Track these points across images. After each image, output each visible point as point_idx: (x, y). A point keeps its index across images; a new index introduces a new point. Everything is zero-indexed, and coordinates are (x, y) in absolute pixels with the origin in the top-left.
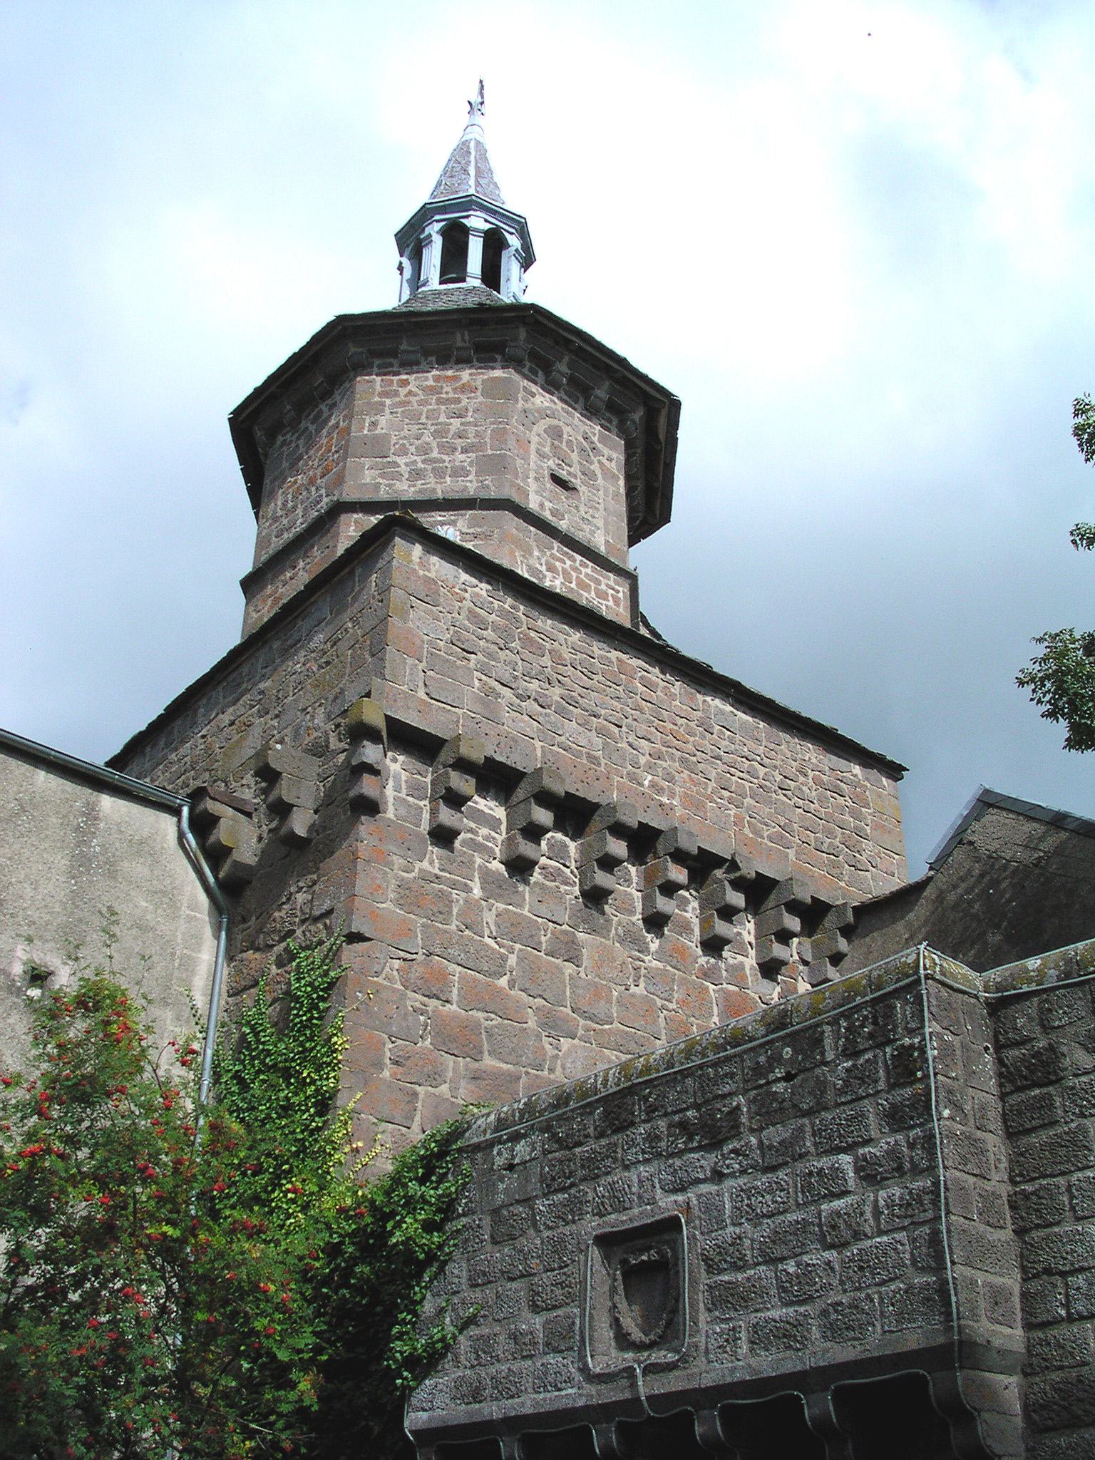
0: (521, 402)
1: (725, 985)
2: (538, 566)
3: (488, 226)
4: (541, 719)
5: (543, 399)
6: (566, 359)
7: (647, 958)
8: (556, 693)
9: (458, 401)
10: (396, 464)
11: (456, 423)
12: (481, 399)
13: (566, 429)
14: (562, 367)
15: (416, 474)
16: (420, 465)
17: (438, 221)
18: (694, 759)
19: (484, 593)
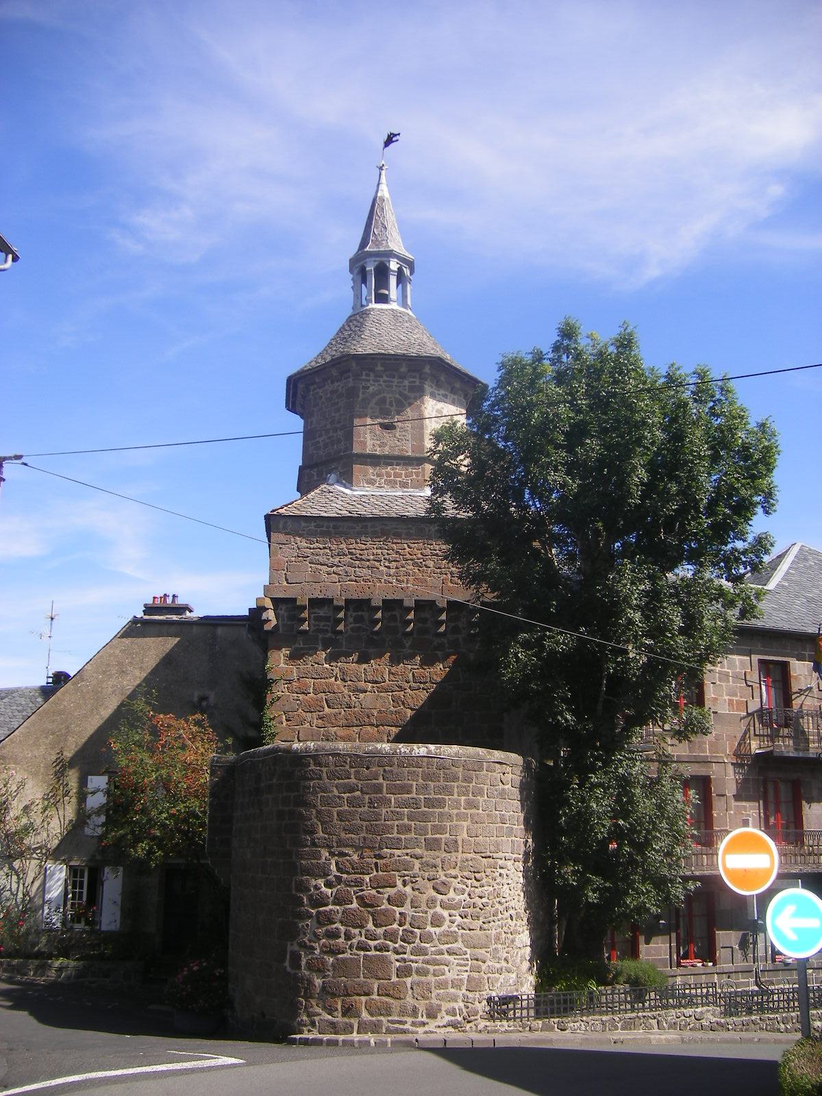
0: (361, 395)
1: (447, 650)
2: (372, 477)
3: (376, 263)
4: (340, 573)
5: (373, 387)
6: (379, 364)
7: (404, 650)
8: (347, 559)
9: (338, 402)
10: (319, 442)
11: (337, 415)
12: (345, 400)
13: (388, 396)
14: (379, 368)
15: (326, 446)
16: (327, 441)
17: (357, 268)
18: (422, 560)
19: (313, 528)
